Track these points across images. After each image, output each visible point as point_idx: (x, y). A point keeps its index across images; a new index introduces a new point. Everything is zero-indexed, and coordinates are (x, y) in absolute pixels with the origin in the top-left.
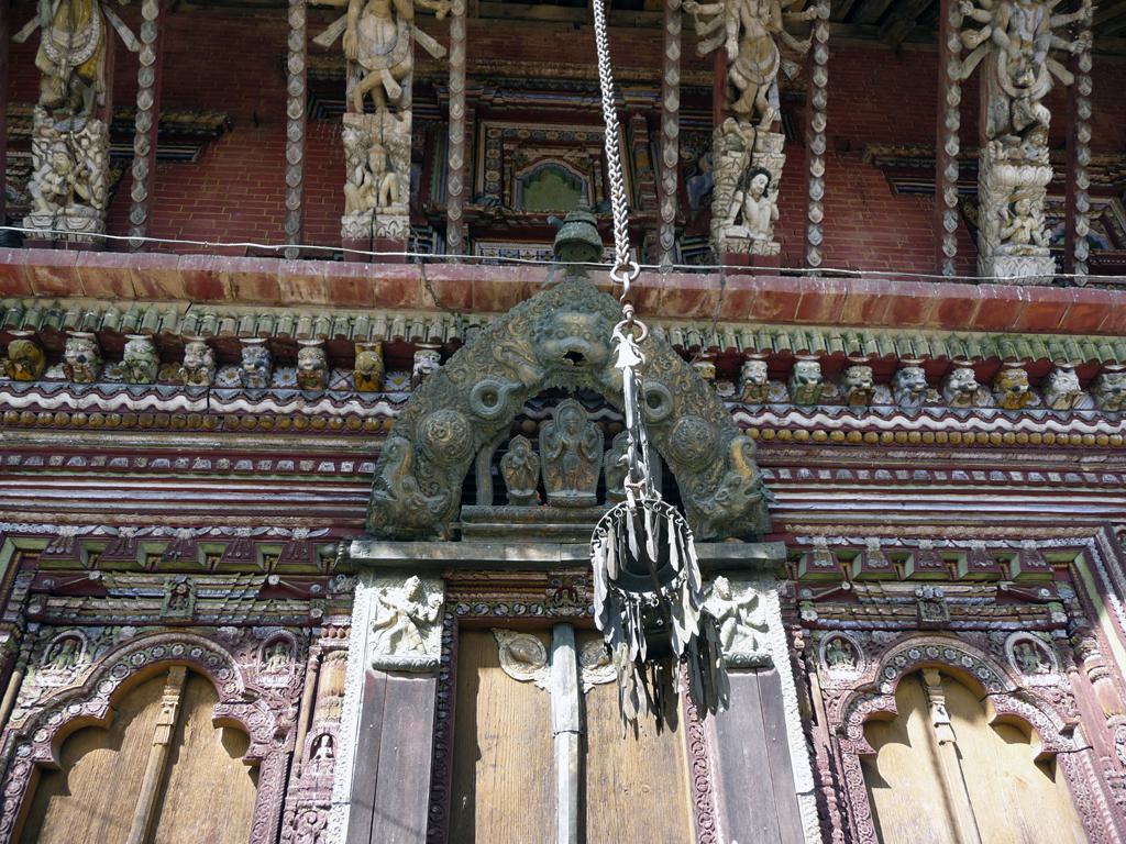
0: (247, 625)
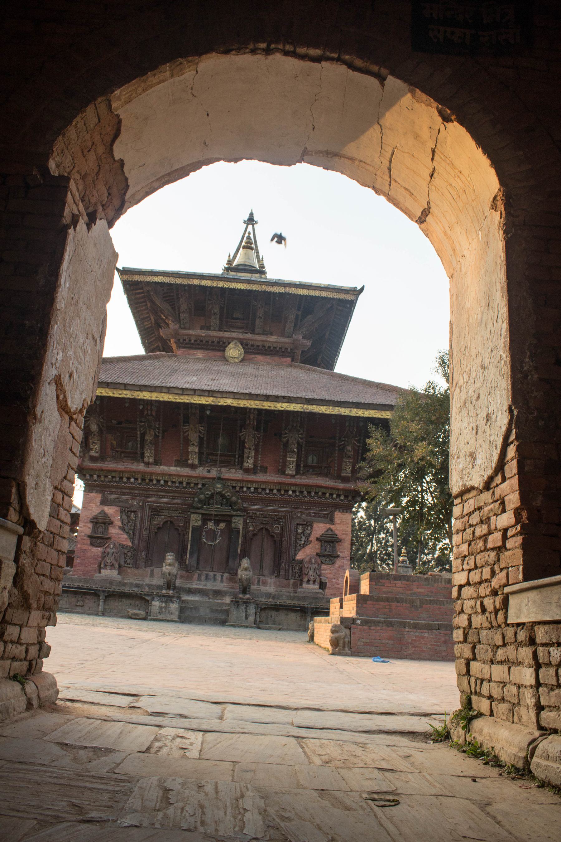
0: (177, 517)
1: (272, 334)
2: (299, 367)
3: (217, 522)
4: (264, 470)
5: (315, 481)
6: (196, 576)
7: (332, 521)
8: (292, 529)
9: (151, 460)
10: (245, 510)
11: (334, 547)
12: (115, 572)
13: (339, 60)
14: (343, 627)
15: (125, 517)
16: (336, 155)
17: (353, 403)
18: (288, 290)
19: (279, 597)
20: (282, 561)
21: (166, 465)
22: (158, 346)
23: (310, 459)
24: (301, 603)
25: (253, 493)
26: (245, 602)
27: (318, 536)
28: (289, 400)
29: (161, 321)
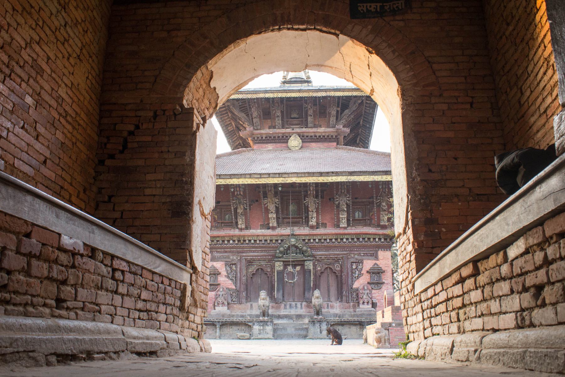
1: (320, 126)
2: (342, 148)
3: (294, 266)
4: (324, 225)
5: (362, 231)
6: (283, 305)
7: (377, 258)
8: (349, 267)
9: (243, 226)
10: (313, 256)
11: (380, 277)
12: (226, 308)
13: (315, 29)
14: (383, 329)
15: (228, 269)
16: (322, 66)
17: (383, 172)
18: (329, 94)
19: (343, 315)
20: (344, 291)
21: (254, 229)
22: (240, 143)
23: (357, 214)
24: (359, 319)
25: (318, 243)
26: (319, 321)
27: (368, 269)
28: (337, 174)
29: (239, 126)
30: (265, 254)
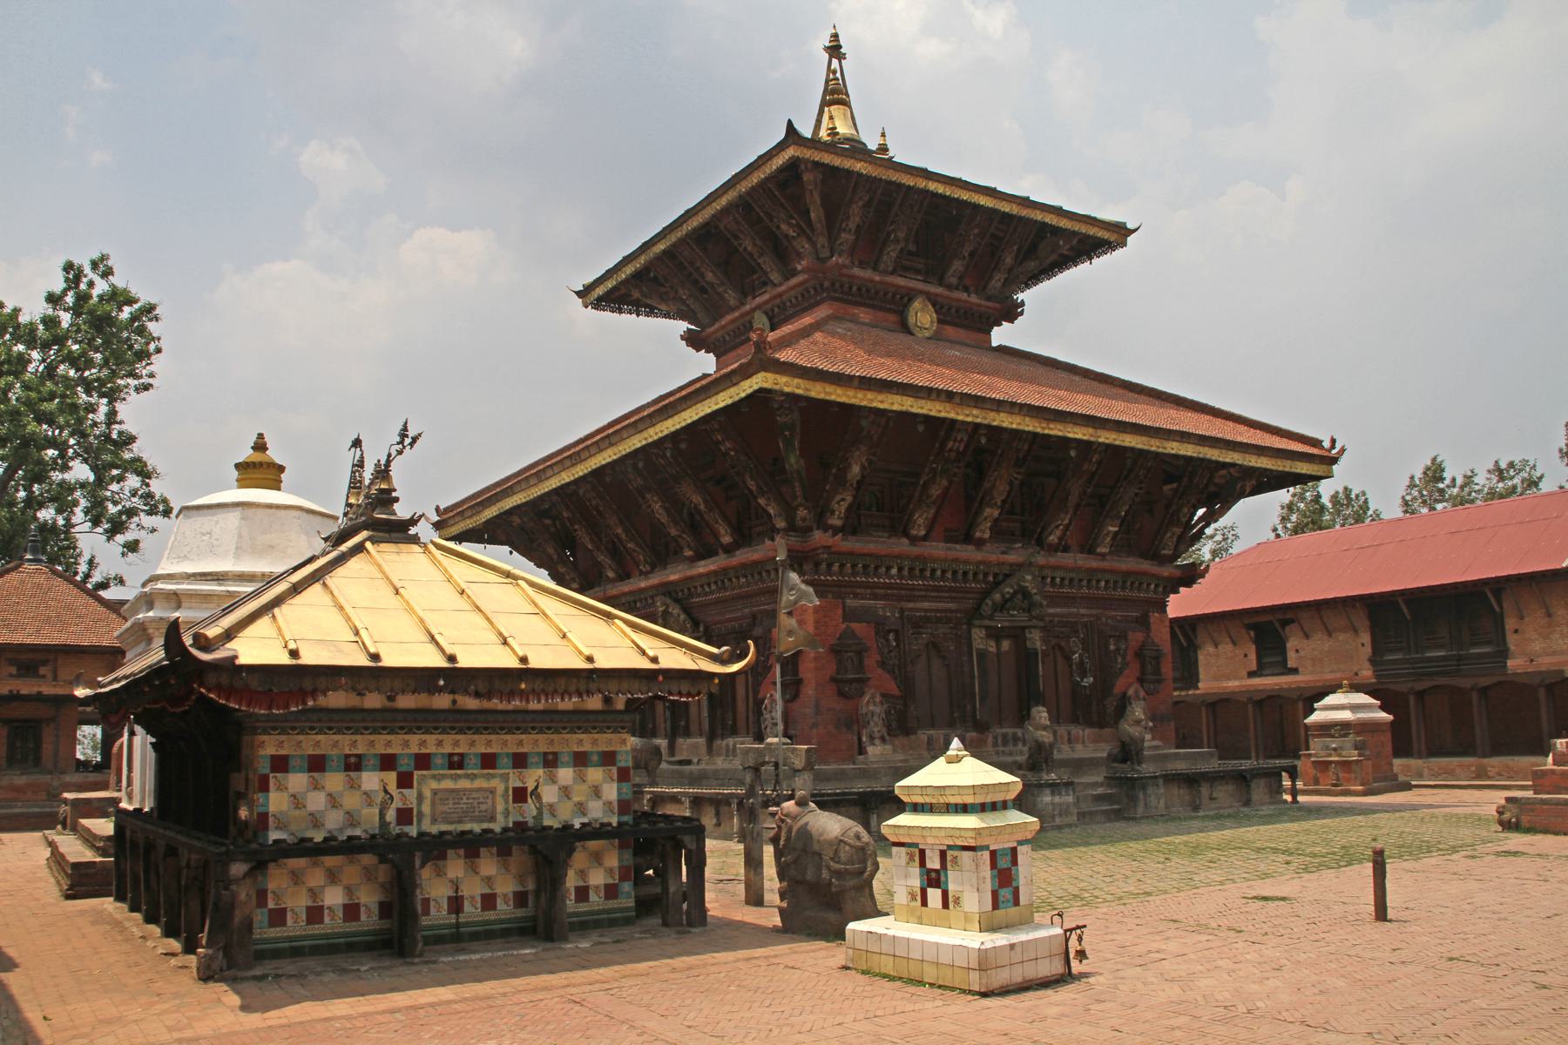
9: (923, 533)
30: (951, 606)
